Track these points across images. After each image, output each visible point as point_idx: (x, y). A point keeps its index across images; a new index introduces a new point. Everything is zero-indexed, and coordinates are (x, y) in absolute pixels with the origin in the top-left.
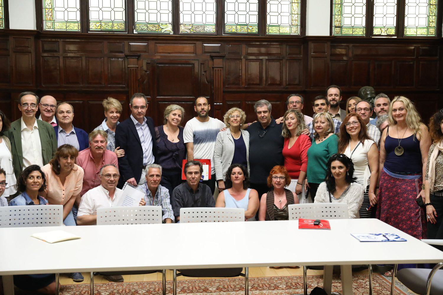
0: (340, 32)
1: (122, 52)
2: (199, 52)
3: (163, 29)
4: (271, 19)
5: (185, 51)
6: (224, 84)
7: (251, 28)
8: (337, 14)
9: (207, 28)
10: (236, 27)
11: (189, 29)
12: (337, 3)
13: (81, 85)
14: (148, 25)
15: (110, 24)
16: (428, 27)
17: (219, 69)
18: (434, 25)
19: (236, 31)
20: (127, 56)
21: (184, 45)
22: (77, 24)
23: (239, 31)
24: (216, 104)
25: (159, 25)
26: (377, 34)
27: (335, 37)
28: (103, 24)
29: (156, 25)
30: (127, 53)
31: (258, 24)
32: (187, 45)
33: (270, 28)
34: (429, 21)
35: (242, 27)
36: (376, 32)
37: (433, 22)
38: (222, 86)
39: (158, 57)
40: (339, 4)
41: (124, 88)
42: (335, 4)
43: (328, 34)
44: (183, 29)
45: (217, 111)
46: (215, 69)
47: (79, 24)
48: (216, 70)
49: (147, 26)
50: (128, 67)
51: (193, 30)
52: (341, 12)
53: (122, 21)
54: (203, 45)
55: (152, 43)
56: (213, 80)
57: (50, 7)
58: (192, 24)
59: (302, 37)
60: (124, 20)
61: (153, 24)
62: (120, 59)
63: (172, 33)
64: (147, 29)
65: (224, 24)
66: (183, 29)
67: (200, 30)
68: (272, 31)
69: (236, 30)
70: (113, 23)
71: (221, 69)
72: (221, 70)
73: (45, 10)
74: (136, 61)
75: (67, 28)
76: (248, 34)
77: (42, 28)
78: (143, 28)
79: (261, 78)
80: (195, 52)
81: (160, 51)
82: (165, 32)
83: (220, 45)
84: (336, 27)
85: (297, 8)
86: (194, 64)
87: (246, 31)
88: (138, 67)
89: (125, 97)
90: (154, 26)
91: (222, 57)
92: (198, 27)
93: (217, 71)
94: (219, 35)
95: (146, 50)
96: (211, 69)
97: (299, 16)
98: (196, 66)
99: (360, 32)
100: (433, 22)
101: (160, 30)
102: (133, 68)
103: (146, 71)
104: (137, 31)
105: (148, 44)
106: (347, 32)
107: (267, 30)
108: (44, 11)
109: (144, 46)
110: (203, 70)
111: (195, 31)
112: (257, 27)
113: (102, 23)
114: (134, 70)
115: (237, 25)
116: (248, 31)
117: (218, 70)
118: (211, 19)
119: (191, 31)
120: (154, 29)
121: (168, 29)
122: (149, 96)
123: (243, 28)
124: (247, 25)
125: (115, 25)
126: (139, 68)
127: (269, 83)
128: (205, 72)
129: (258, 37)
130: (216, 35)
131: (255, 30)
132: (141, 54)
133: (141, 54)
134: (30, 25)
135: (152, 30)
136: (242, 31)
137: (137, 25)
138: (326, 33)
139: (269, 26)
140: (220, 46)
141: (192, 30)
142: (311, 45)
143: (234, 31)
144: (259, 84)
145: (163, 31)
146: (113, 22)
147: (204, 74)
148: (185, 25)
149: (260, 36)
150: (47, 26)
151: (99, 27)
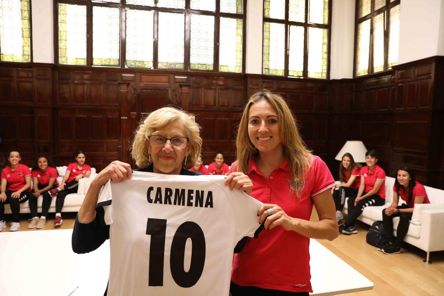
0: (268, 73)
1: (116, 81)
2: (172, 81)
3: (146, 65)
4: (221, 62)
5: (162, 81)
6: (189, 106)
7: (208, 67)
8: (266, 60)
9: (178, 65)
10: (198, 65)
11: (165, 66)
12: (266, 53)
13: (86, 104)
14: (136, 62)
15: (108, 61)
16: (322, 73)
17: (187, 94)
18: (325, 71)
19: (198, 68)
20: (119, 84)
21: (161, 77)
22: (84, 60)
23: (200, 69)
25: (143, 62)
26: (291, 75)
27: (265, 75)
28: (103, 61)
29: (141, 62)
30: (120, 81)
31: (214, 64)
32: (163, 77)
33: (221, 67)
34: (322, 69)
35: (202, 65)
36: (290, 73)
37: (325, 70)
38: (188, 106)
39: (142, 85)
40: (267, 54)
41: (117, 106)
42: (265, 54)
43: (260, 73)
44: (160, 66)
46: (183, 94)
47: (86, 60)
48: (183, 95)
49: (135, 63)
50: (120, 92)
52: (269, 59)
53: (117, 58)
54: (174, 77)
55: (138, 74)
57: (65, 48)
58: (167, 62)
59: (243, 74)
60: (119, 58)
61: (140, 62)
62: (115, 86)
63: (152, 68)
64: (135, 65)
65: (190, 63)
66: (160, 66)
67: (173, 67)
68: (223, 69)
69: (198, 68)
70: (110, 60)
72: (187, 95)
73: (61, 50)
74: (127, 87)
76: (207, 71)
77: (58, 62)
78: (132, 64)
79: (215, 102)
80: (169, 82)
81: (144, 80)
82: (148, 67)
83: (186, 77)
84: (265, 69)
85: (240, 56)
86: (168, 91)
87: (205, 68)
88: (127, 92)
89: (118, 113)
90: (140, 63)
91: (188, 86)
92: (171, 64)
94: (186, 70)
95: (134, 79)
96: (180, 94)
97: (242, 60)
98: (170, 91)
99: (281, 73)
100: (325, 70)
103: (134, 95)
104: (127, 66)
105: (135, 76)
106: (272, 73)
107: (219, 69)
108: (59, 50)
109: (132, 77)
110: (174, 95)
111: (169, 67)
112: (212, 66)
113: (102, 60)
115: (199, 64)
117: (185, 95)
118: (181, 59)
119: (166, 67)
120: (140, 65)
121: (150, 65)
122: (135, 112)
124: (205, 64)
125: (112, 61)
127: (221, 104)
128: (176, 96)
129: (213, 73)
130: (184, 70)
131: (211, 68)
132: (130, 82)
133: (130, 82)
134: (49, 59)
135: (138, 66)
136: (202, 68)
137: (128, 62)
138: (259, 72)
139: (221, 66)
140: (186, 79)
142: (249, 80)
143: (196, 68)
144: (213, 106)
145: (146, 67)
146: (110, 59)
148: (162, 63)
149: (215, 72)
150: (62, 61)
151: (100, 63)
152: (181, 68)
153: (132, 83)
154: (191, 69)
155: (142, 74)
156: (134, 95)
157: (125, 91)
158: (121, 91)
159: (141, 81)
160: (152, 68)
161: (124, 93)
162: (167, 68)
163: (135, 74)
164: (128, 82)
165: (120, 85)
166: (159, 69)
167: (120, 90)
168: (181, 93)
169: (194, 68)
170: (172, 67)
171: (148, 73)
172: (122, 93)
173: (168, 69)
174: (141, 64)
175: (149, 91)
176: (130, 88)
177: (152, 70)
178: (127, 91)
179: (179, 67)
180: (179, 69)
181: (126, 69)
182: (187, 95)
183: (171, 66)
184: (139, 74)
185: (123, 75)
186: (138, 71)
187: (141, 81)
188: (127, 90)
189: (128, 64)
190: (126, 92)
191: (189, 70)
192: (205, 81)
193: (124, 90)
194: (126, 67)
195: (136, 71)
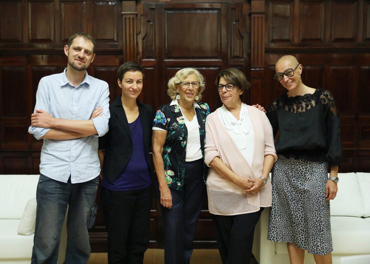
24: (254, 69)
45: (256, 80)
46: (253, 16)
48: (254, 18)
50: (122, 15)
56: (250, 34)
62: (110, 3)
71: (263, 16)
72: (262, 17)
88: (137, 15)
93: (256, 19)
96: (247, 17)
102: (129, 16)
114: (131, 18)
117: (258, 17)
122: (152, 58)
126: (139, 15)
128: (237, 21)
147: (236, 23)
156: (149, 21)
168: (250, 15)
172: (125, 18)
178: (137, 13)
182: (262, 17)
188: (136, 11)
190: (133, 14)
193: (130, 11)
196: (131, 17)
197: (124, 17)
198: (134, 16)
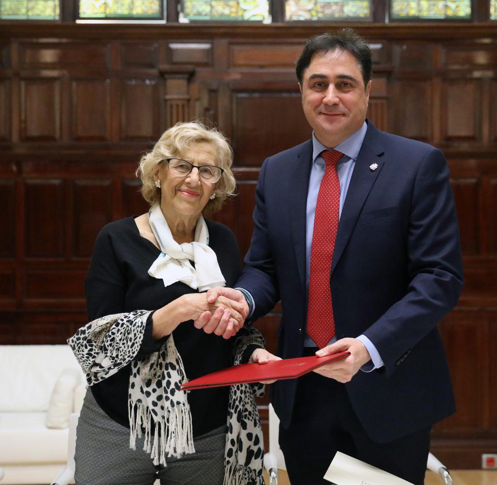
1: (151, 66)
11: (310, 11)
17: (379, 101)
20: (162, 75)
30: (165, 67)
39: (235, 75)
50: (166, 101)
51: (317, 12)
62: (148, 82)
63: (268, 21)
64: (211, 12)
71: (384, 101)
75: (30, 13)
76: (448, 20)
78: (200, 9)
81: (242, 62)
87: (443, 12)
88: (189, 100)
90: (228, 5)
95: (208, 60)
101: (240, 13)
104: (186, 16)
109: (203, 51)
116: (446, 14)
117: (376, 105)
119: (312, 16)
120: (227, 11)
123: (434, 5)
135: (222, 15)
141: (314, 13)
149: (476, 23)
151: (102, 10)
152: (362, 15)
153: (201, 72)
154: (394, 17)
155: (234, 40)
157: (181, 97)
158: (168, 97)
159: (231, 64)
160: (268, 21)
161: (177, 106)
162: (315, 19)
163: (212, 44)
164: (190, 68)
165: (165, 80)
166: (289, 22)
167: (166, 94)
169: (403, 14)
170: (332, 15)
171: (255, 36)
172: (171, 106)
173: (318, 21)
174: (231, 7)
175: (256, 95)
176: (195, 87)
177: (267, 27)
179: (355, 12)
180: (353, 18)
181: (184, 27)
183: (328, 11)
184: (224, 42)
185: (174, 46)
186: (222, 31)
187: (231, 64)
189: (187, 10)
191: (387, 21)
192: (439, 55)
194: (183, 20)
195: (216, 31)
196: (180, 103)
197: (169, 103)
198: (185, 103)
